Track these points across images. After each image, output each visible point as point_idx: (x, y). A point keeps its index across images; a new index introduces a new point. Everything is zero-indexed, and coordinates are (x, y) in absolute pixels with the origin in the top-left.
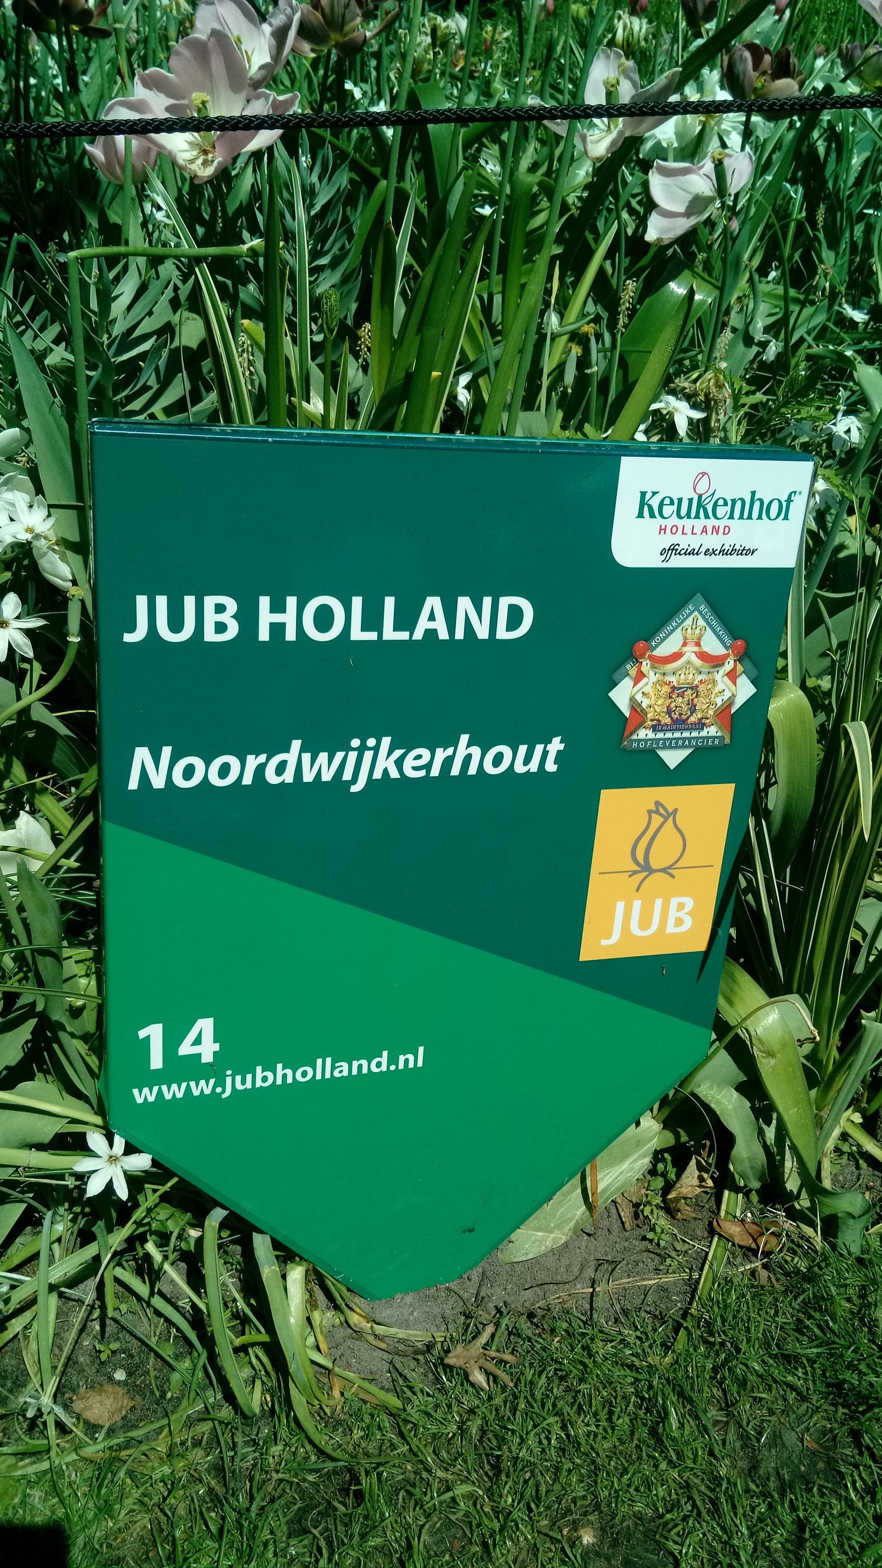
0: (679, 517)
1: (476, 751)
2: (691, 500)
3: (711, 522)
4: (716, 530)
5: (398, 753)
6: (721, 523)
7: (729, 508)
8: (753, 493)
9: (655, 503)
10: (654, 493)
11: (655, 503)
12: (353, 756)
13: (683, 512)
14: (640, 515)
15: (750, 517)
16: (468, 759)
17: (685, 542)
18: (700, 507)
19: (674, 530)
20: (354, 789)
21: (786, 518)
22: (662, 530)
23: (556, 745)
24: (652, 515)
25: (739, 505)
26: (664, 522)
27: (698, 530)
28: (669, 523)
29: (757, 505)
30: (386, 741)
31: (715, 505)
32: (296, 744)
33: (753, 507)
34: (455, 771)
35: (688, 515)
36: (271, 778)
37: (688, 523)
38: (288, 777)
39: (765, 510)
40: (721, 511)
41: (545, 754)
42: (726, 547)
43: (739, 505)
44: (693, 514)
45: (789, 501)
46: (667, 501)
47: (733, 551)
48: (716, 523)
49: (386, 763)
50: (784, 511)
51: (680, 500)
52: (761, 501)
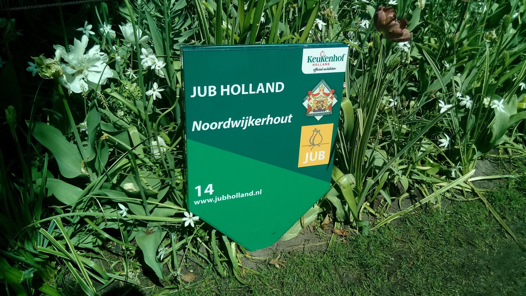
1: (272, 119)
4: (326, 64)
5: (254, 120)
6: (327, 63)
9: (311, 59)
11: (311, 59)
12: (243, 121)
14: (308, 62)
16: (270, 120)
17: (319, 67)
18: (322, 59)
19: (316, 65)
20: (244, 129)
22: (314, 65)
23: (291, 116)
28: (315, 63)
30: (251, 117)
32: (230, 119)
33: (335, 58)
34: (267, 123)
36: (224, 127)
37: (319, 63)
38: (228, 127)
39: (337, 59)
40: (327, 60)
41: (288, 118)
45: (343, 56)
47: (330, 69)
49: (251, 122)
50: (342, 59)
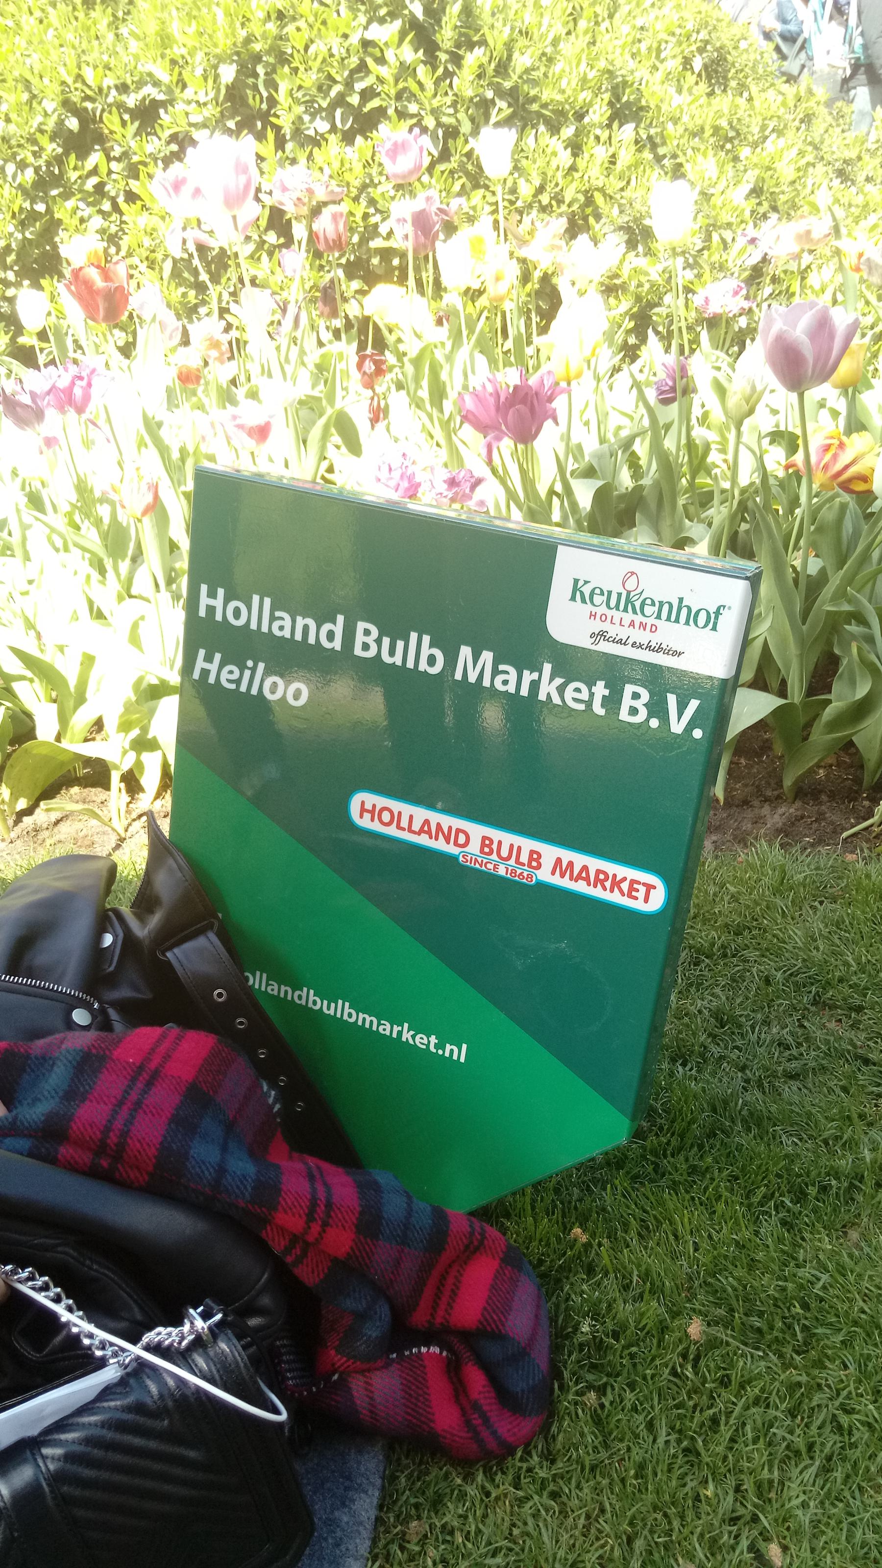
2: (620, 595)
3: (639, 618)
4: (643, 626)
7: (656, 609)
8: (681, 600)
9: (587, 590)
10: (586, 582)
11: (587, 590)
13: (613, 603)
14: (573, 599)
17: (613, 631)
18: (629, 602)
19: (604, 618)
21: (714, 628)
22: (593, 615)
24: (583, 601)
25: (666, 608)
26: (594, 610)
27: (626, 622)
29: (684, 611)
31: (643, 604)
33: (679, 612)
37: (617, 615)
39: (692, 617)
40: (648, 610)
42: (653, 644)
43: (666, 608)
44: (622, 607)
46: (598, 591)
47: (659, 649)
48: (645, 620)
51: (610, 593)
52: (689, 609)
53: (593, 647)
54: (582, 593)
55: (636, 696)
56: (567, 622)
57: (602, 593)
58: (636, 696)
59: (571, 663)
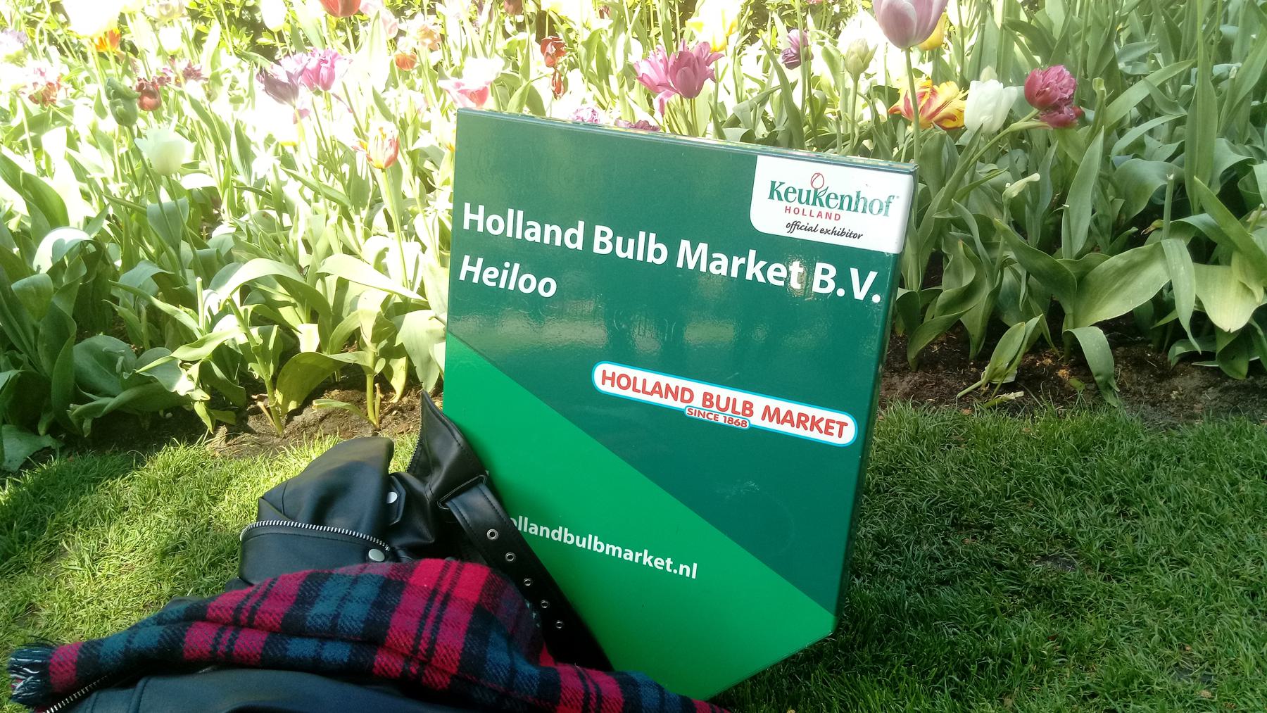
0: (800, 202)
2: (809, 192)
3: (825, 210)
4: (829, 216)
6: (836, 211)
7: (839, 201)
8: (858, 193)
9: (782, 190)
11: (782, 190)
13: (804, 199)
14: (771, 197)
15: (856, 210)
17: (804, 221)
18: (816, 197)
19: (797, 211)
21: (886, 214)
22: (788, 210)
25: (846, 200)
26: (789, 205)
35: (807, 201)
37: (808, 208)
40: (832, 203)
42: (837, 230)
43: (846, 200)
44: (811, 201)
47: (843, 233)
48: (830, 211)
51: (801, 191)
53: (789, 235)
54: (779, 193)
55: (825, 272)
56: (767, 216)
57: (795, 191)
58: (825, 272)
59: (775, 249)
